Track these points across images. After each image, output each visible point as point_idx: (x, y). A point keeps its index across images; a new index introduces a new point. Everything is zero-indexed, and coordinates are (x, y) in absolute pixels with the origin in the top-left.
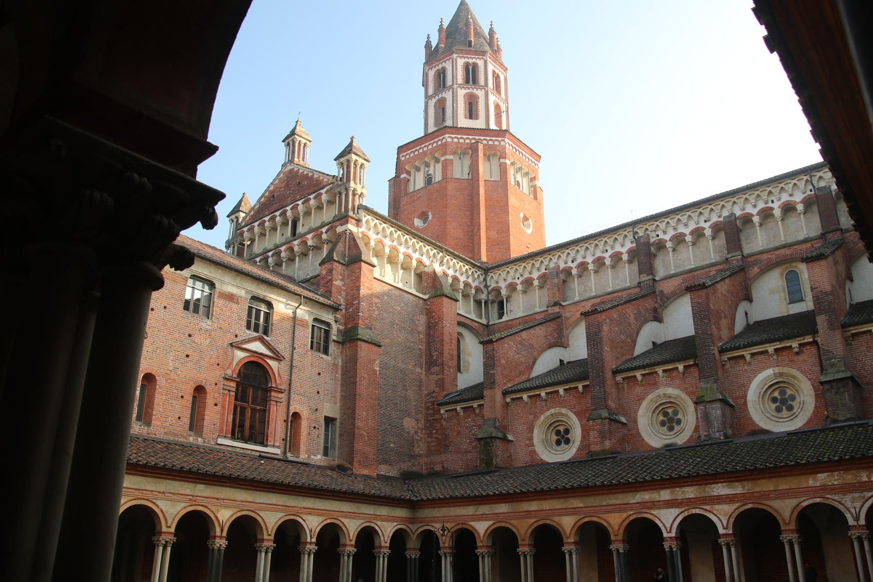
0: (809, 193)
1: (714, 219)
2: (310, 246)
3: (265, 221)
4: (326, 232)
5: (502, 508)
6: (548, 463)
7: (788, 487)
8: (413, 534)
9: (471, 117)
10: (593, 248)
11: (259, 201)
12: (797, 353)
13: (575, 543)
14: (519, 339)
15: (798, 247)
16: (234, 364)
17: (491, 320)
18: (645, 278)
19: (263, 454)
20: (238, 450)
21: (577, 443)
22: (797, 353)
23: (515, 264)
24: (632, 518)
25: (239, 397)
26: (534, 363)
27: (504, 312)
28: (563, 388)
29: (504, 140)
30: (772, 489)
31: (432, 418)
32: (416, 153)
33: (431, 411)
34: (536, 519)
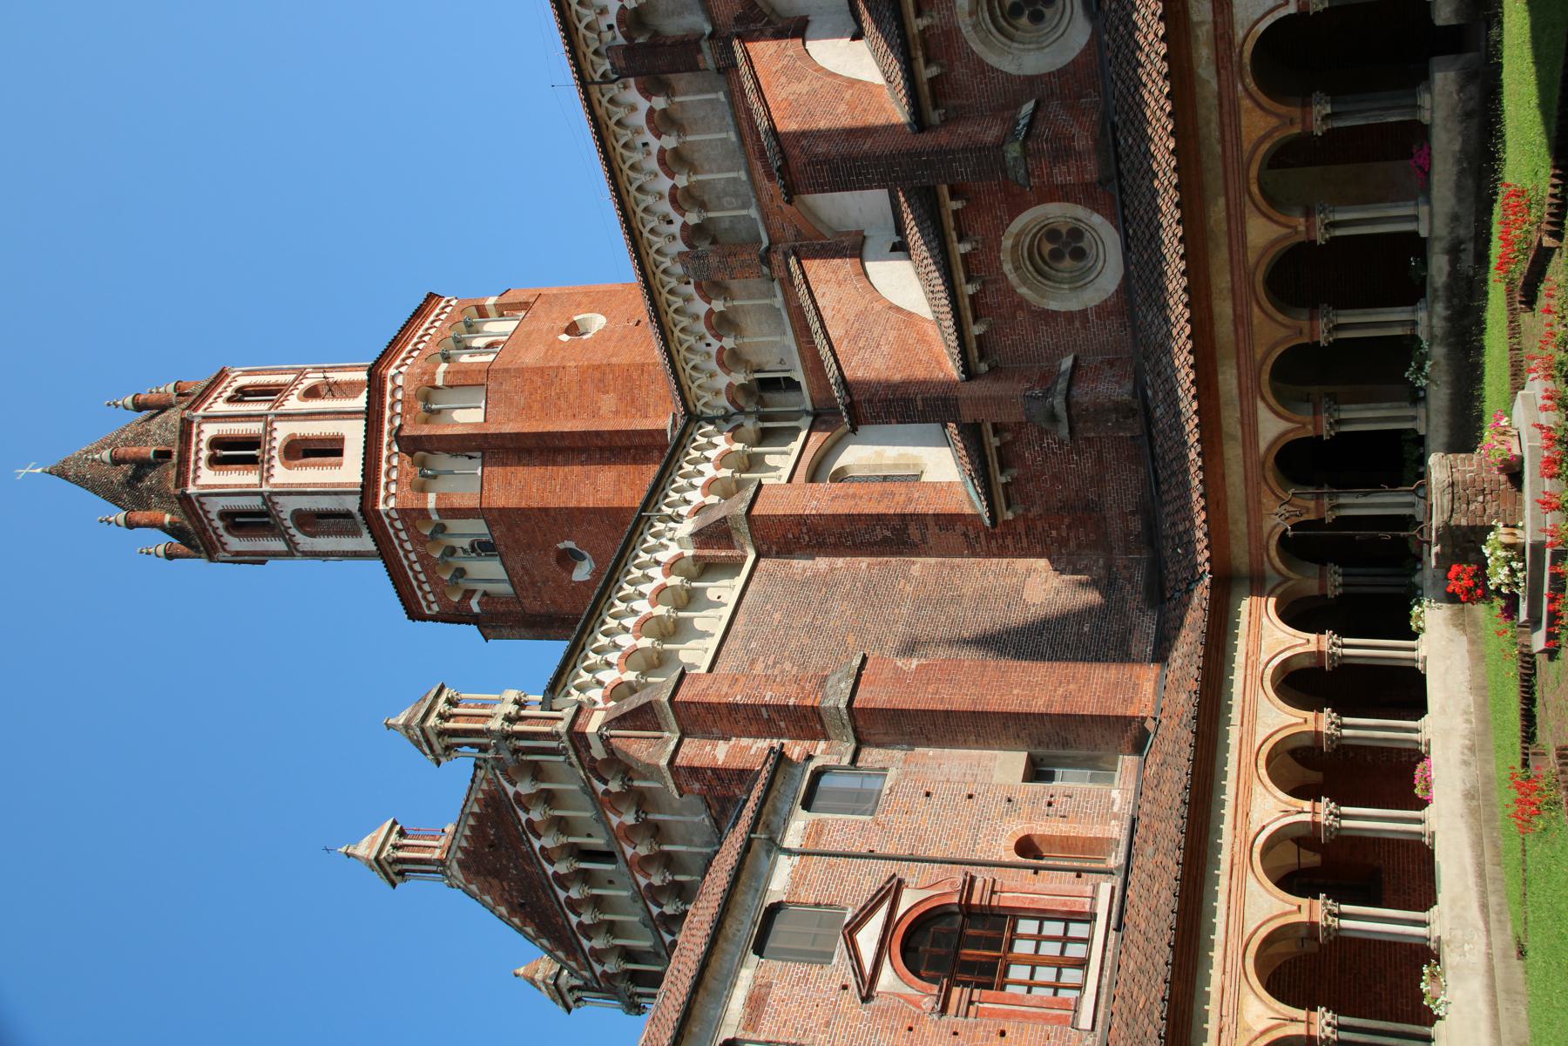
2: (637, 820)
3: (580, 924)
4: (606, 782)
5: (1228, 380)
6: (1126, 277)
8: (1287, 579)
9: (339, 452)
10: (638, 176)
11: (533, 940)
13: (1308, 213)
14: (845, 343)
16: (909, 991)
17: (802, 408)
19: (1113, 923)
20: (1105, 981)
21: (1080, 211)
23: (675, 352)
24: (1252, 86)
25: (984, 979)
26: (899, 309)
27: (785, 378)
28: (956, 244)
29: (393, 378)
31: (1024, 537)
32: (422, 577)
33: (1009, 541)
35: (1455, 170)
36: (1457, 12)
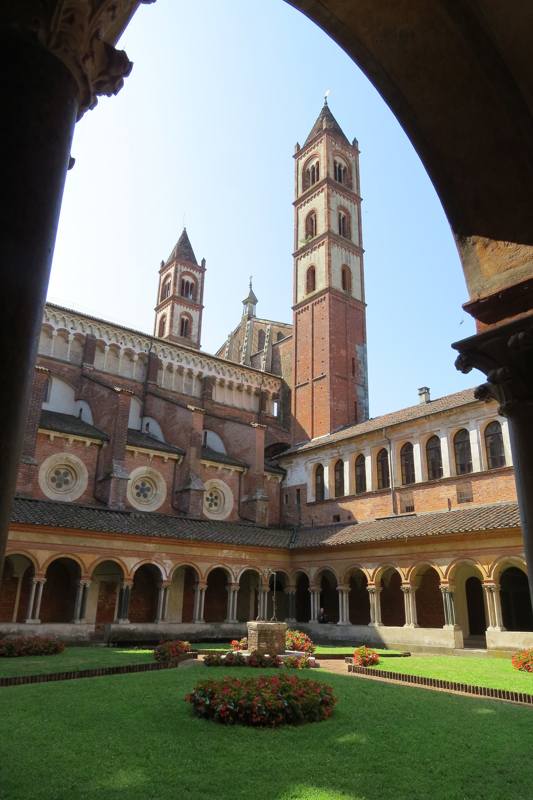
0: (144, 352)
1: (79, 330)
7: (207, 555)
12: (164, 463)
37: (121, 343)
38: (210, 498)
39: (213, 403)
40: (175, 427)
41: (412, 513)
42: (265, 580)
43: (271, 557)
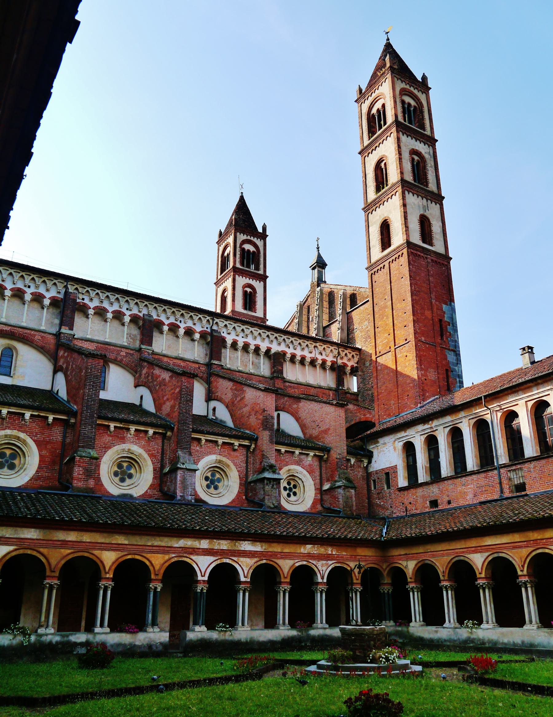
1: (135, 311)
5: (31, 534)
12: (235, 450)
15: (190, 364)
18: (65, 330)
22: (235, 450)
24: (173, 560)
30: (279, 551)
34: (72, 551)
35: (127, 642)
36: (191, 640)
37: (181, 322)
38: (288, 487)
39: (284, 380)
40: (244, 409)
41: (523, 493)
42: (356, 578)
43: (362, 552)
